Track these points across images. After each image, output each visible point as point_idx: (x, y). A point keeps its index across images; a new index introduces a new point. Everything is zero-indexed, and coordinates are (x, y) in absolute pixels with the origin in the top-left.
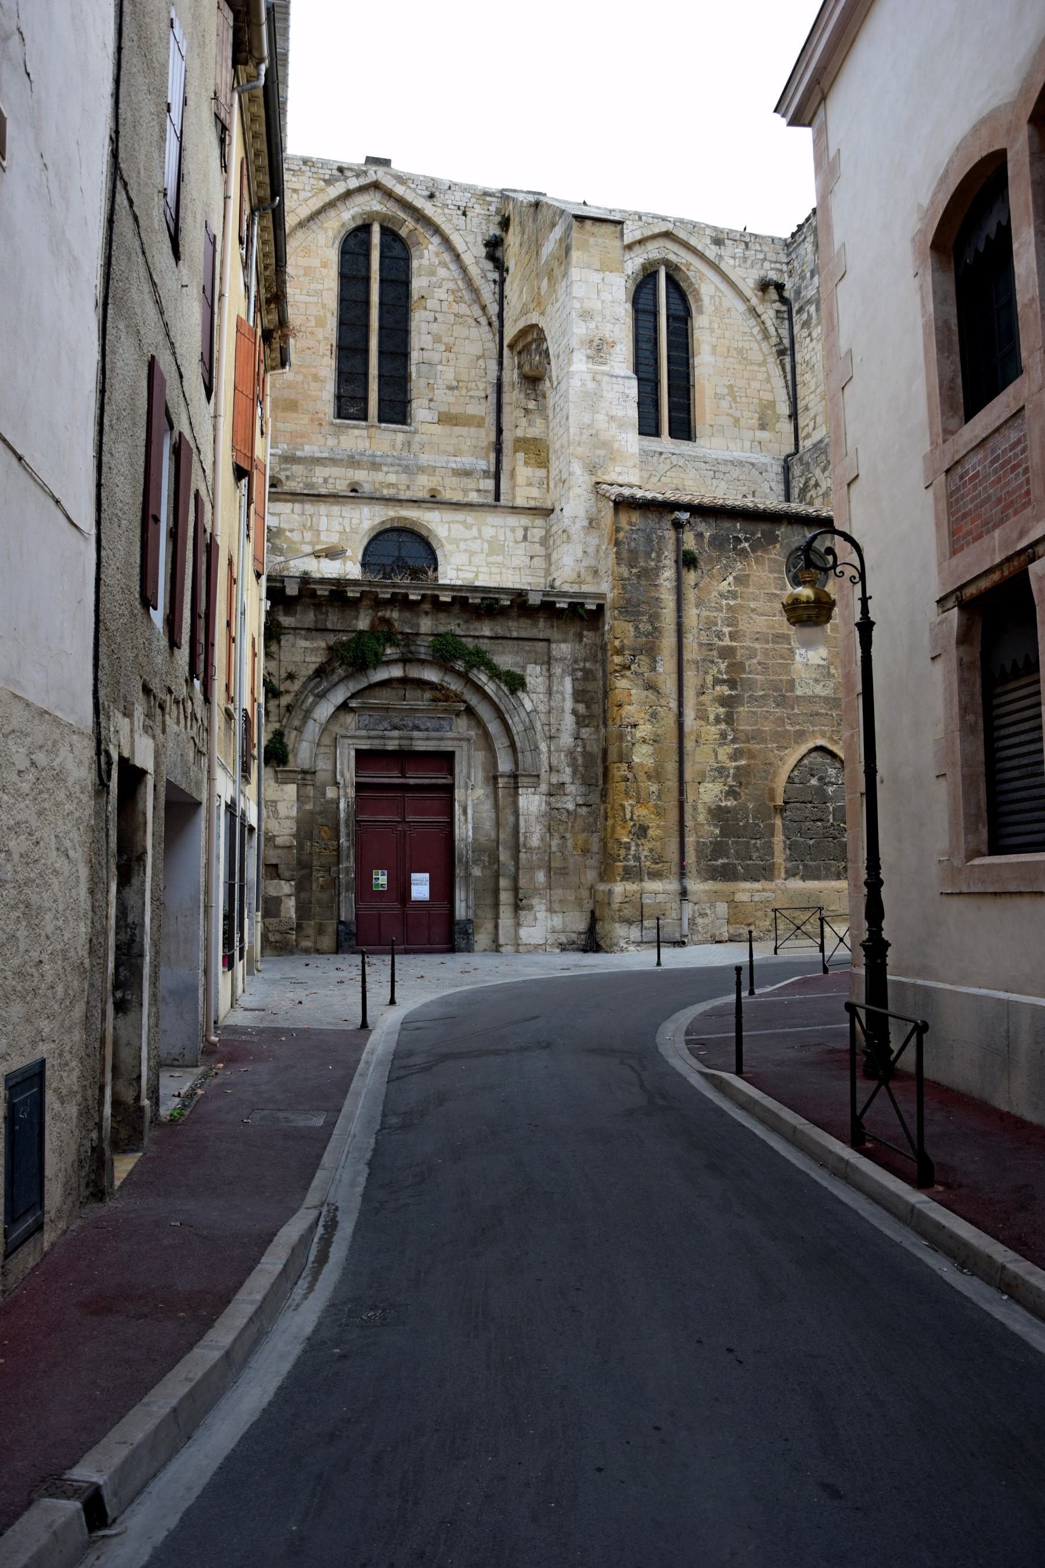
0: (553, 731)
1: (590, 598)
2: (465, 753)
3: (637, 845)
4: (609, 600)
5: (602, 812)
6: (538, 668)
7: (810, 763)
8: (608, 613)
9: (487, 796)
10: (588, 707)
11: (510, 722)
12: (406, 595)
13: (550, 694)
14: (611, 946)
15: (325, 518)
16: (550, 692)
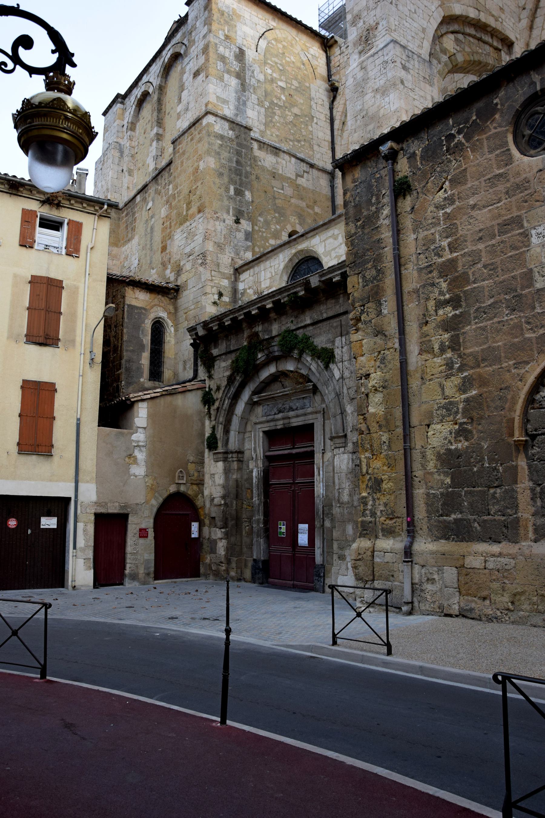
3: (374, 500)
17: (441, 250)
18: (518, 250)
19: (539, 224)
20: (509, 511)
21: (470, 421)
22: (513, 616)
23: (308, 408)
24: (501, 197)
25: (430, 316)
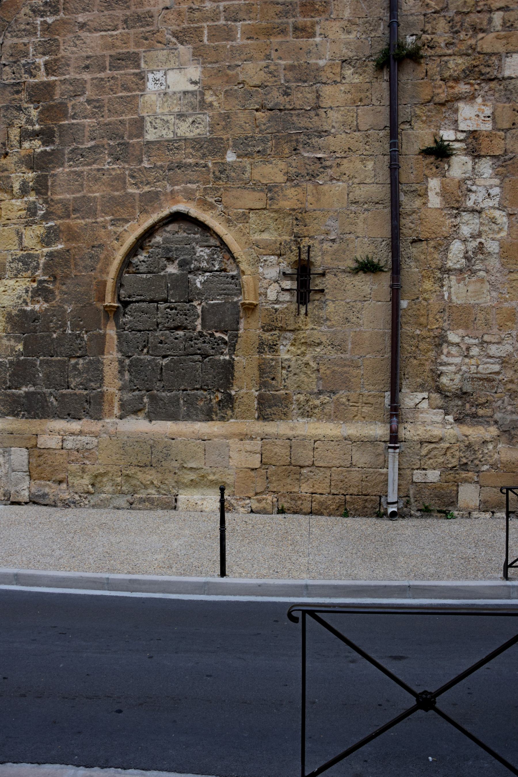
7: (166, 240)
17: (35, 68)
18: (130, 91)
19: (158, 68)
20: (92, 384)
21: (52, 279)
22: (94, 500)
24: (117, 25)
25: (12, 146)
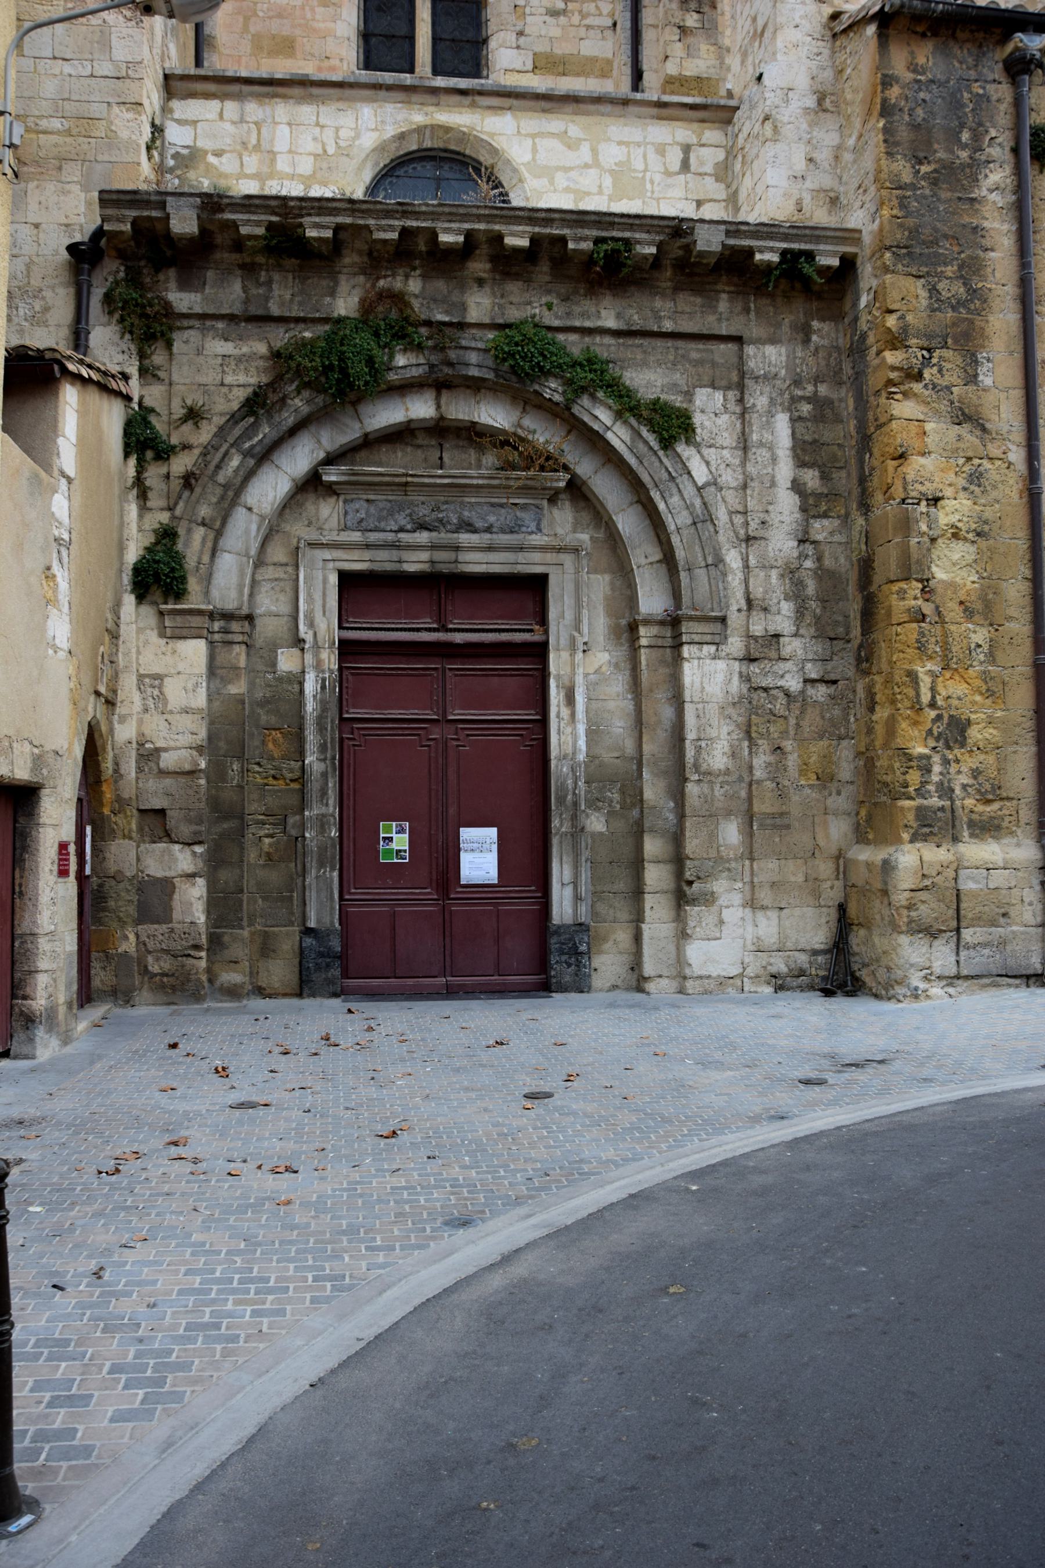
0: (753, 525)
1: (826, 239)
2: (569, 577)
3: (946, 762)
4: (867, 238)
5: (861, 693)
6: (719, 396)
8: (867, 277)
9: (616, 666)
10: (825, 477)
11: (662, 506)
12: (433, 234)
13: (745, 449)
14: (889, 985)
15: (286, 129)
16: (744, 445)
23: (532, 533)
